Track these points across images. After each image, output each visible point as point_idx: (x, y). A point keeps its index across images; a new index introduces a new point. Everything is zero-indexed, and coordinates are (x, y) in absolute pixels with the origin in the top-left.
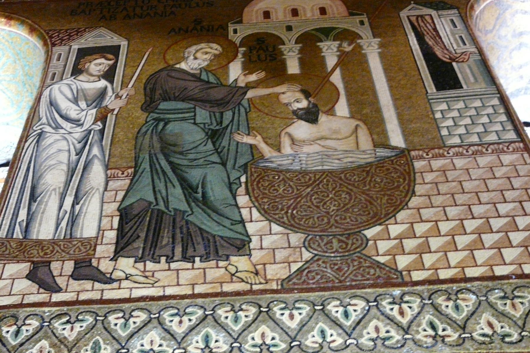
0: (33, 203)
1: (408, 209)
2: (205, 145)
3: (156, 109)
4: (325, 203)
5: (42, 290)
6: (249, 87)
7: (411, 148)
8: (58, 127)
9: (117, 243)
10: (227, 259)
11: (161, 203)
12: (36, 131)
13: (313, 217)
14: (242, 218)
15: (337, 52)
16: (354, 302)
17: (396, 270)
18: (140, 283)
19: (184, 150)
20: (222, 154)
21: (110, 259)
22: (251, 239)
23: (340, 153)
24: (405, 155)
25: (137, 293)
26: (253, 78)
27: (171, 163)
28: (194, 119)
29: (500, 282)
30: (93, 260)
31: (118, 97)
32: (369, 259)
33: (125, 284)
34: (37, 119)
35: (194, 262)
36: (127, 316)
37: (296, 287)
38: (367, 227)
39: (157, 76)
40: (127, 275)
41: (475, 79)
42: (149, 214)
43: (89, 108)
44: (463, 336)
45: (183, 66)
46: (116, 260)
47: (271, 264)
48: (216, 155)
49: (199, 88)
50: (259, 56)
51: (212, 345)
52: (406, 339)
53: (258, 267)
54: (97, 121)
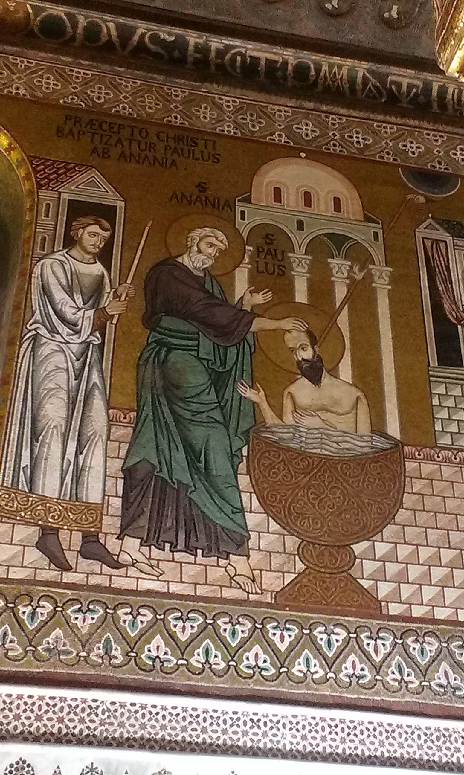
0: (35, 443)
1: (394, 524)
2: (208, 394)
3: (158, 326)
4: (320, 501)
5: (52, 566)
6: (254, 313)
7: (405, 442)
8: (53, 331)
9: (123, 517)
10: (227, 558)
11: (165, 470)
12: (30, 331)
14: (242, 505)
15: (347, 278)
16: (337, 630)
18: (145, 573)
21: (116, 536)
22: (250, 535)
23: (340, 434)
26: (260, 298)
27: (173, 412)
28: (198, 351)
30: (100, 535)
31: (117, 296)
32: (354, 582)
33: (132, 571)
35: (196, 556)
36: (135, 613)
37: (288, 603)
38: (356, 541)
40: (133, 559)
45: (185, 260)
46: (122, 539)
47: (266, 570)
48: (219, 410)
49: (201, 303)
50: (267, 264)
51: (212, 660)
53: (256, 573)
54: (96, 330)
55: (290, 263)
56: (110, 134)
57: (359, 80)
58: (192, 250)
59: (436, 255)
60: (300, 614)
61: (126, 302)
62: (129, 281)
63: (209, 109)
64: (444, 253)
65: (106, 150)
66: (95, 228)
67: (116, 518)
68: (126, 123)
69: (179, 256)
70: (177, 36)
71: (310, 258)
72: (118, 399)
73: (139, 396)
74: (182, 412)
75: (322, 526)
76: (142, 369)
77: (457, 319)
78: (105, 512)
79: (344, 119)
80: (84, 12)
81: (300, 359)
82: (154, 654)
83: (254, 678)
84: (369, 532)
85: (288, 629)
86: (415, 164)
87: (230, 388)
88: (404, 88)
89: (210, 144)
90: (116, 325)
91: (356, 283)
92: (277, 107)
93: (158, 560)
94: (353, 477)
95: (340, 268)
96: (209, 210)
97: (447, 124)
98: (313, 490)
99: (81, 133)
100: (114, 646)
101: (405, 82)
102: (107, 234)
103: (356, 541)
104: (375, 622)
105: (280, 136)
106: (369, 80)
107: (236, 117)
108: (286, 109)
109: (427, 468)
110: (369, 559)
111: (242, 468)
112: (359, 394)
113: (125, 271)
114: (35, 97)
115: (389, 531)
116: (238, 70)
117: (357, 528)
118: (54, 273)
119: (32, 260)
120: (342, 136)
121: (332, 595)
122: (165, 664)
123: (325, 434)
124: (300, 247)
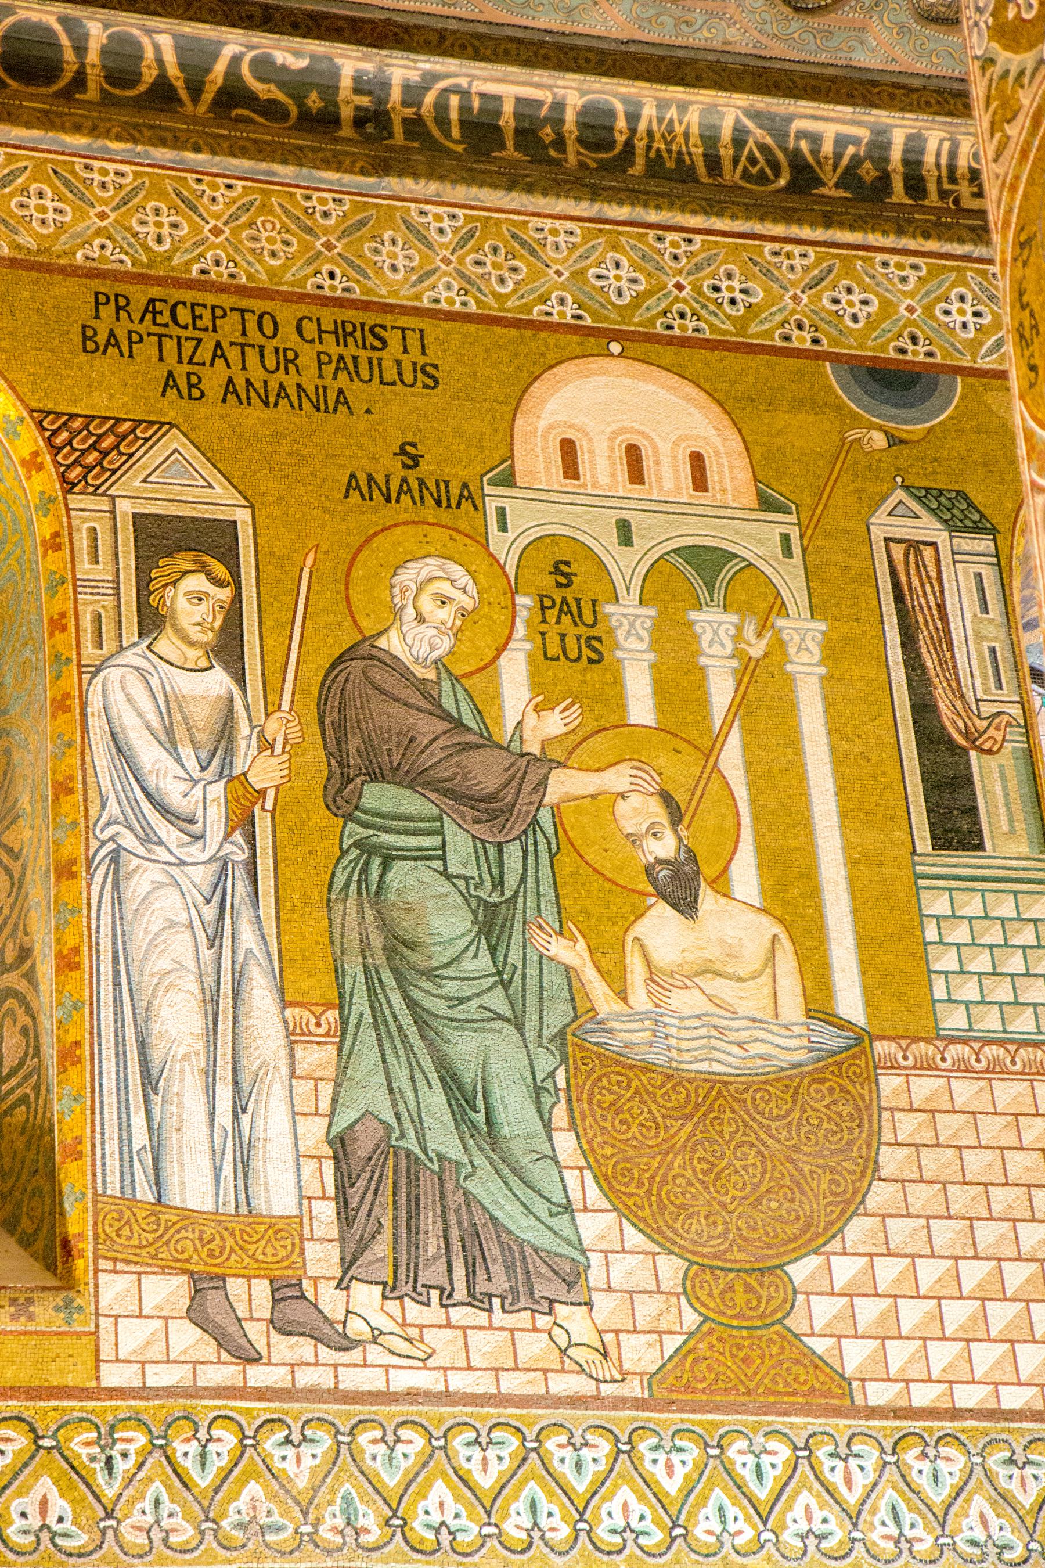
0: (152, 1096)
1: (866, 1215)
2: (475, 956)
3: (356, 808)
5: (225, 1356)
7: (875, 1031)
8: (149, 838)
9: (342, 1239)
11: (411, 1133)
12: (103, 843)
13: (698, 1213)
17: (842, 1376)
19: (434, 963)
20: (511, 991)
21: (335, 1283)
23: (745, 1023)
24: (863, 1051)
25: (402, 1380)
26: (554, 724)
27: (411, 1004)
28: (443, 858)
29: (1006, 1425)
30: (305, 1282)
31: (266, 745)
33: (375, 1353)
34: (98, 801)
35: (490, 1310)
36: (390, 1438)
37: (674, 1396)
38: (794, 1256)
39: (342, 678)
41: (1011, 821)
42: (390, 1163)
43: (209, 775)
44: (941, 1541)
45: (392, 643)
46: (347, 1288)
49: (441, 743)
50: (563, 636)
51: (544, 1522)
52: (854, 1540)
53: (609, 1338)
54: (234, 829)
55: (611, 631)
56: (198, 334)
57: (726, 134)
58: (405, 618)
59: (916, 582)
60: (698, 1417)
61: (286, 756)
62: (285, 706)
63: (400, 243)
64: (933, 574)
65: (194, 380)
66: (197, 582)
67: (330, 1246)
68: (227, 301)
69: (381, 633)
70: (313, 57)
71: (652, 612)
72: (300, 984)
73: (339, 973)
74: (429, 1003)
75: (727, 1231)
76: (338, 908)
77: (966, 735)
78: (307, 1233)
79: (698, 238)
80: (102, 13)
81: (652, 860)
82: (436, 1519)
83: (627, 1552)
84: (818, 1235)
85: (680, 1450)
86: (861, 346)
87: (517, 938)
88: (828, 148)
89: (413, 338)
90: (273, 813)
91: (753, 663)
92: (548, 224)
93: (421, 1327)
94: (779, 1118)
95: (715, 632)
96: (430, 512)
97: (926, 236)
98: (700, 1153)
99: (135, 338)
100: (362, 1508)
101: (829, 131)
102: (225, 594)
103: (794, 1256)
104: (842, 1422)
105: (562, 301)
106: (748, 132)
107: (461, 261)
108: (570, 225)
109: (924, 1087)
110: (821, 1294)
111: (560, 1116)
112: (778, 929)
113: (274, 681)
114: (19, 247)
115: (857, 1230)
116: (456, 133)
117: (792, 1230)
118: (129, 700)
119: (80, 673)
120: (698, 290)
121: (755, 1373)
122: (460, 1537)
123: (715, 1027)
124: (628, 589)
